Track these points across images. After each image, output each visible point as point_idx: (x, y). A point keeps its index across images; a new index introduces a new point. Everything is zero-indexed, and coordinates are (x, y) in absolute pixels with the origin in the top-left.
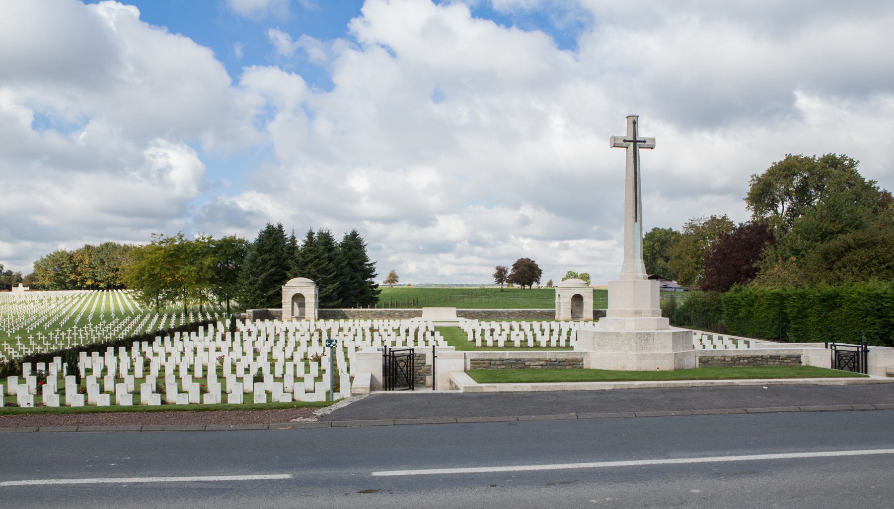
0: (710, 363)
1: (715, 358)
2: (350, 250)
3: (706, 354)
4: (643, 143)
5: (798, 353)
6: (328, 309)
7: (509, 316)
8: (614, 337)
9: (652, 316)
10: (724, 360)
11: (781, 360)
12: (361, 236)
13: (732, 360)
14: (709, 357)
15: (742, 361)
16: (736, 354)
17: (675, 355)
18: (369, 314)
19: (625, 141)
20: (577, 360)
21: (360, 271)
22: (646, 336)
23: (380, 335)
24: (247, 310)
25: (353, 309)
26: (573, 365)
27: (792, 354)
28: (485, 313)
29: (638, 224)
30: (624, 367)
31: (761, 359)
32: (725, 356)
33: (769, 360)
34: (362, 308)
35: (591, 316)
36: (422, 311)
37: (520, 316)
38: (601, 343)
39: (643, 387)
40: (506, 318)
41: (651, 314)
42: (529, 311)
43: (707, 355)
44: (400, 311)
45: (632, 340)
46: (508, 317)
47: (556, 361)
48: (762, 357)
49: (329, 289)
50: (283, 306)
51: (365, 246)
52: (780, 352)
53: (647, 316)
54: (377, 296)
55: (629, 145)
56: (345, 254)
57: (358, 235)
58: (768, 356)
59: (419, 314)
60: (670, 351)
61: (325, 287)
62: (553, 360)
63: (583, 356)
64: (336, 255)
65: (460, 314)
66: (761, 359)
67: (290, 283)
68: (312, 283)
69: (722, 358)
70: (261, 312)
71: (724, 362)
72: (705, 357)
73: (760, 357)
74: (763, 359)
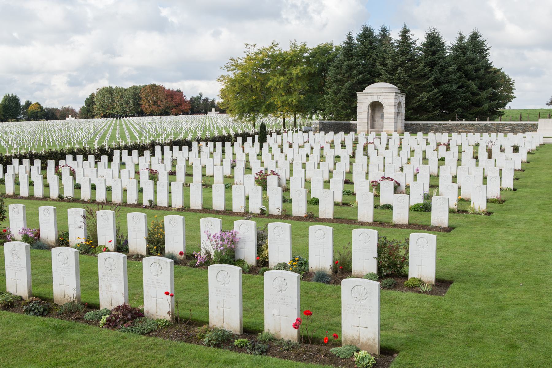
2: (464, 53)
12: (482, 38)
18: (470, 128)
21: (476, 78)
25: (450, 122)
44: (511, 125)
49: (423, 98)
51: (488, 49)
56: (456, 58)
59: (534, 128)
61: (419, 96)
64: (440, 58)
67: (369, 89)
68: (395, 88)
70: (336, 124)
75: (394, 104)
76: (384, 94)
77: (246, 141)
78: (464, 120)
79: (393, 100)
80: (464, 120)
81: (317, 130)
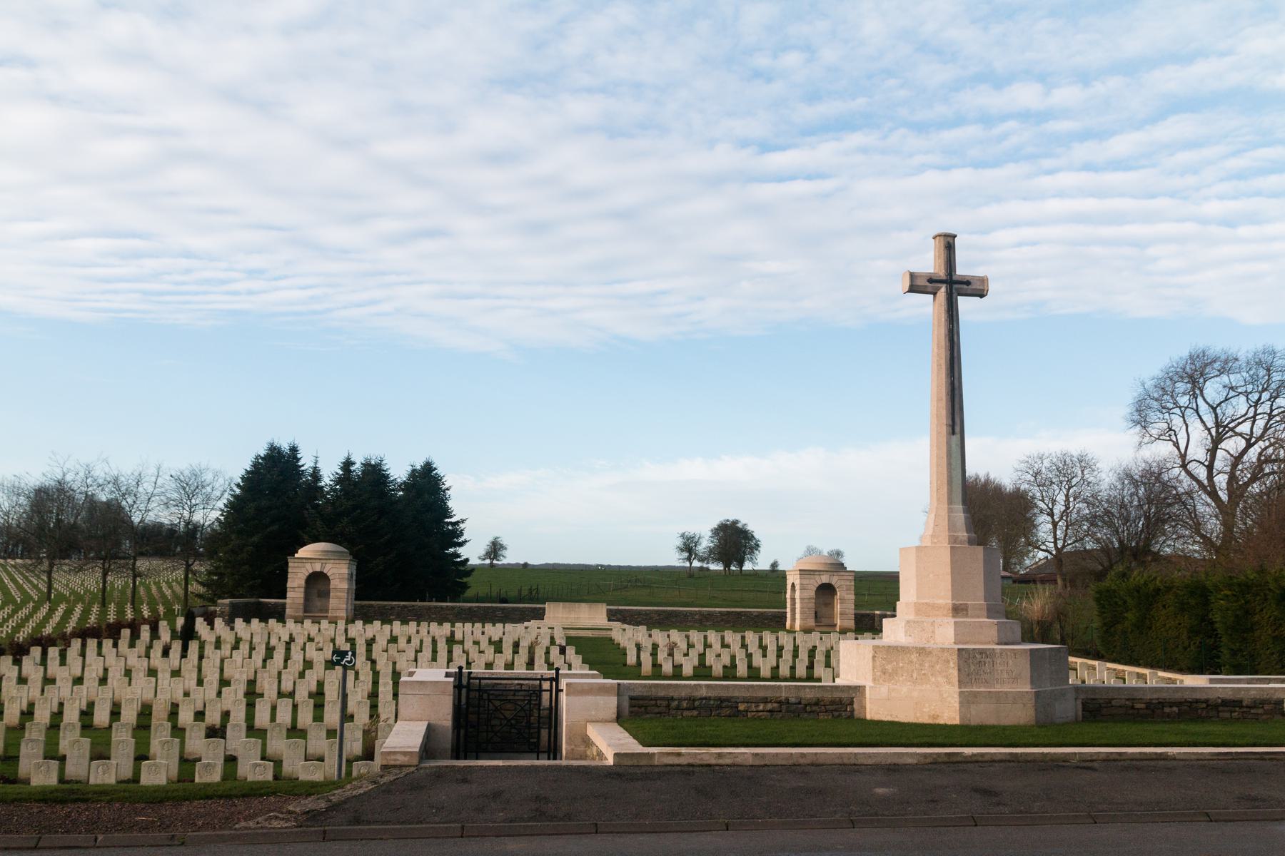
0: (1104, 711)
1: (1114, 703)
4: (965, 287)
6: (373, 602)
7: (703, 622)
8: (914, 657)
9: (988, 618)
10: (1133, 708)
11: (1245, 710)
12: (440, 471)
13: (1147, 708)
14: (1101, 701)
15: (1167, 710)
18: (448, 612)
19: (931, 281)
20: (840, 701)
22: (977, 656)
23: (464, 652)
24: (219, 601)
26: (832, 711)
27: (1265, 696)
28: (659, 615)
29: (957, 437)
30: (935, 717)
31: (1204, 705)
32: (1134, 699)
33: (1221, 708)
34: (437, 601)
35: (851, 623)
36: (544, 609)
37: (722, 620)
38: (889, 667)
39: (980, 759)
40: (697, 625)
41: (985, 613)
42: (739, 613)
43: (1097, 697)
45: (952, 665)
46: (701, 622)
47: (800, 703)
48: (1206, 701)
50: (289, 595)
51: (447, 489)
53: (978, 617)
54: (465, 580)
55: (939, 289)
57: (435, 469)
58: (1220, 701)
59: (540, 615)
60: (1027, 688)
62: (793, 700)
63: (854, 695)
65: (614, 616)
66: (1204, 705)
67: (303, 552)
69: (1127, 703)
70: (246, 604)
71: (1131, 712)
72: (1094, 699)
74: (1208, 706)
75: (346, 576)
76: (332, 561)
77: (139, 637)
78: (434, 599)
79: (346, 571)
80: (434, 599)
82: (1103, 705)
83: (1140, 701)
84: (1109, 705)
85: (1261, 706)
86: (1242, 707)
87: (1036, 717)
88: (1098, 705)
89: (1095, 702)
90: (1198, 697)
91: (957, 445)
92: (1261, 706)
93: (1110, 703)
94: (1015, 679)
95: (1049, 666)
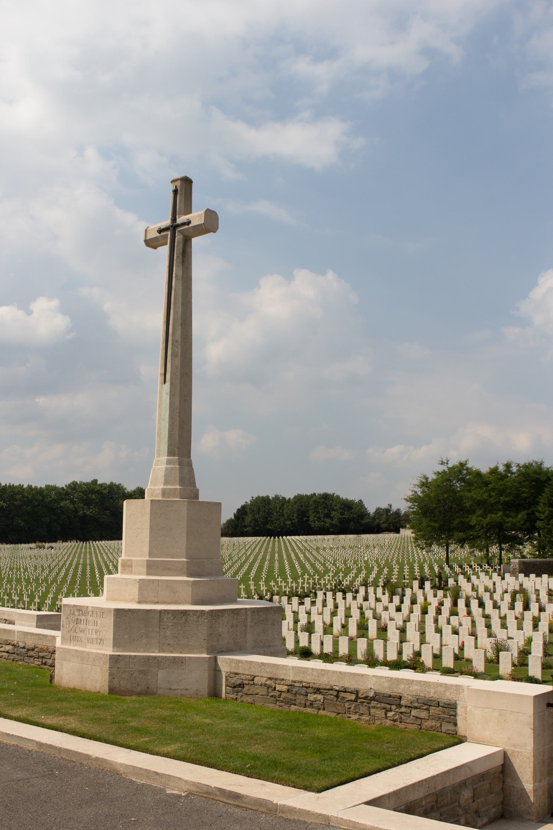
3: (239, 667)
5: (448, 696)
11: (403, 709)
13: (288, 691)
14: (243, 677)
15: (311, 697)
16: (298, 678)
17: (114, 660)
22: (77, 613)
26: (43, 657)
32: (276, 679)
33: (373, 703)
41: (145, 570)
43: (240, 671)
48: (357, 692)
52: (402, 686)
66: (353, 697)
72: (236, 674)
73: (351, 692)
74: (357, 697)
81: (516, 572)
82: (245, 682)
83: (283, 682)
84: (251, 682)
85: (425, 707)
86: (400, 706)
87: (110, 682)
88: (239, 682)
89: (238, 676)
90: (346, 686)
91: (167, 394)
92: (425, 707)
93: (253, 680)
94: (101, 641)
95: (158, 630)
